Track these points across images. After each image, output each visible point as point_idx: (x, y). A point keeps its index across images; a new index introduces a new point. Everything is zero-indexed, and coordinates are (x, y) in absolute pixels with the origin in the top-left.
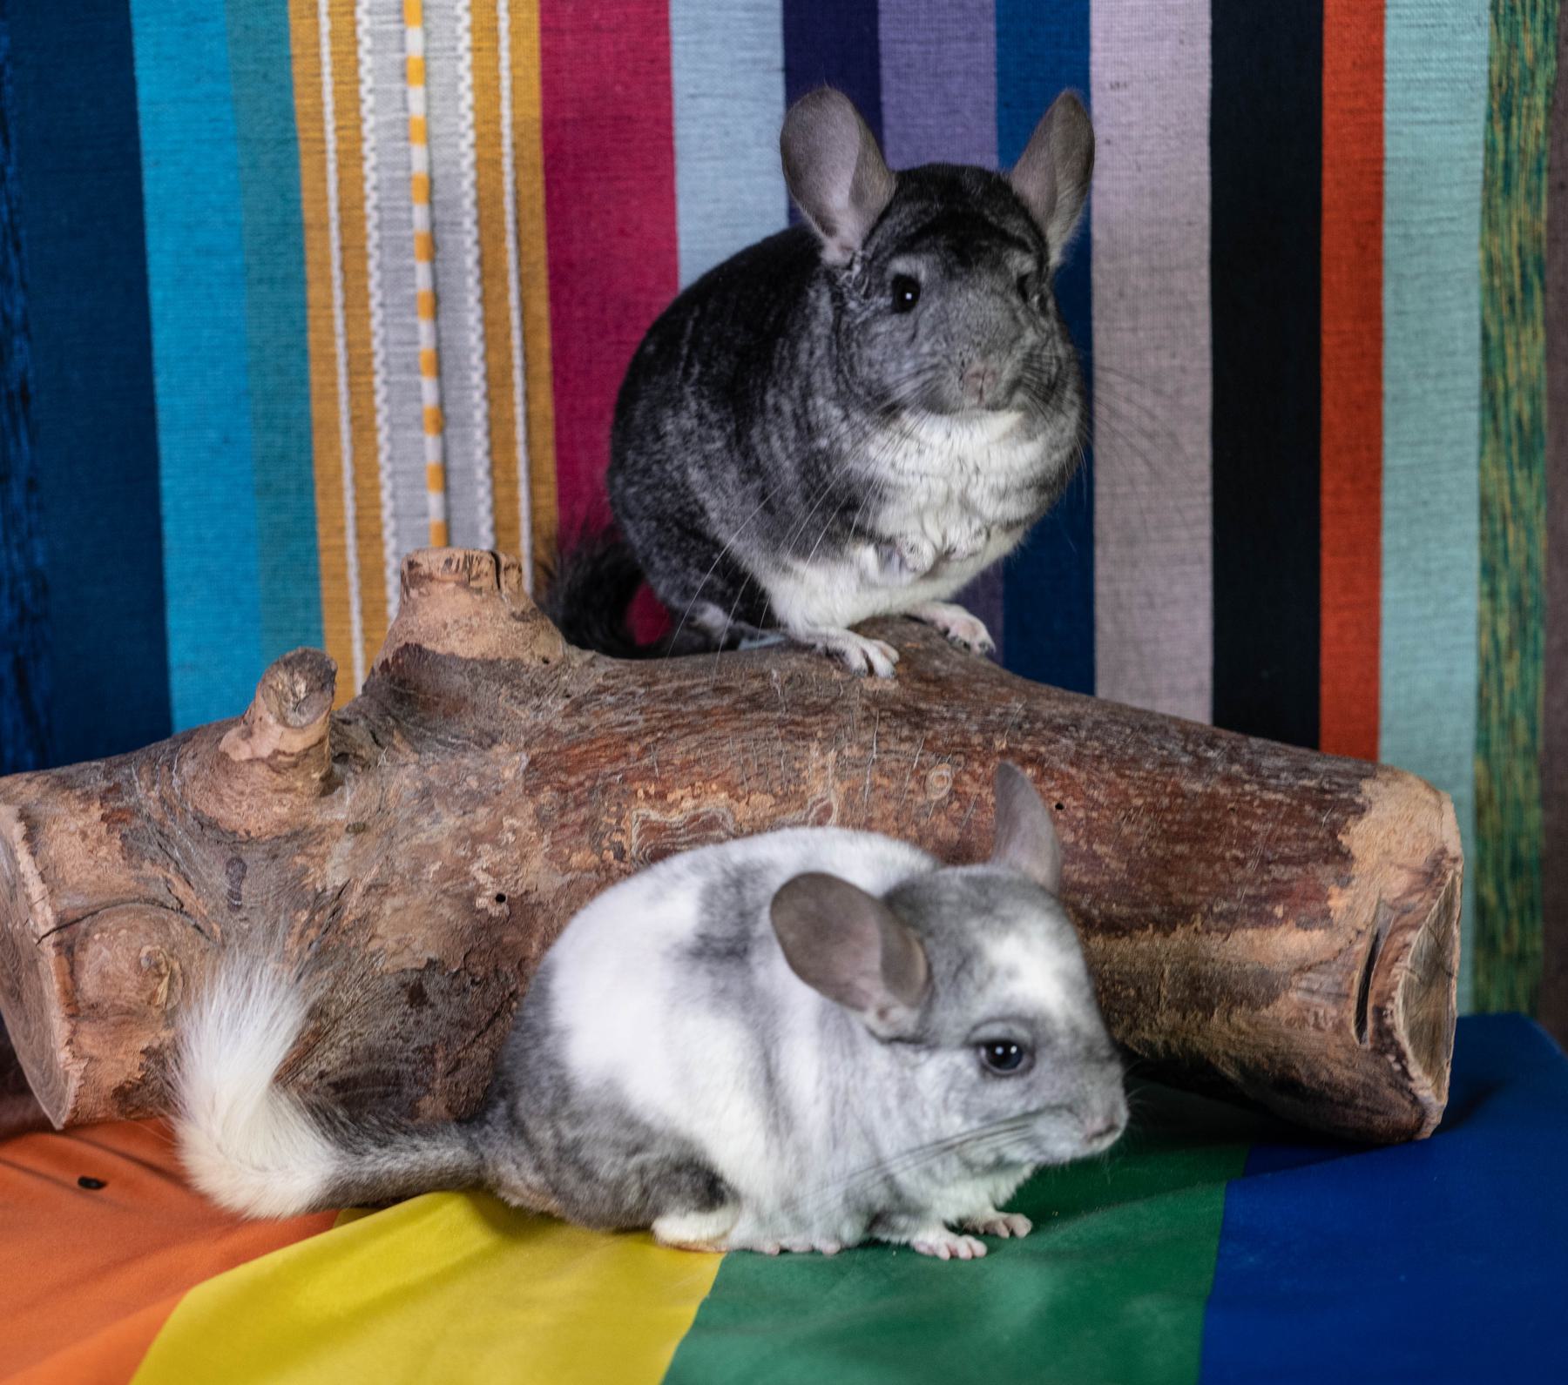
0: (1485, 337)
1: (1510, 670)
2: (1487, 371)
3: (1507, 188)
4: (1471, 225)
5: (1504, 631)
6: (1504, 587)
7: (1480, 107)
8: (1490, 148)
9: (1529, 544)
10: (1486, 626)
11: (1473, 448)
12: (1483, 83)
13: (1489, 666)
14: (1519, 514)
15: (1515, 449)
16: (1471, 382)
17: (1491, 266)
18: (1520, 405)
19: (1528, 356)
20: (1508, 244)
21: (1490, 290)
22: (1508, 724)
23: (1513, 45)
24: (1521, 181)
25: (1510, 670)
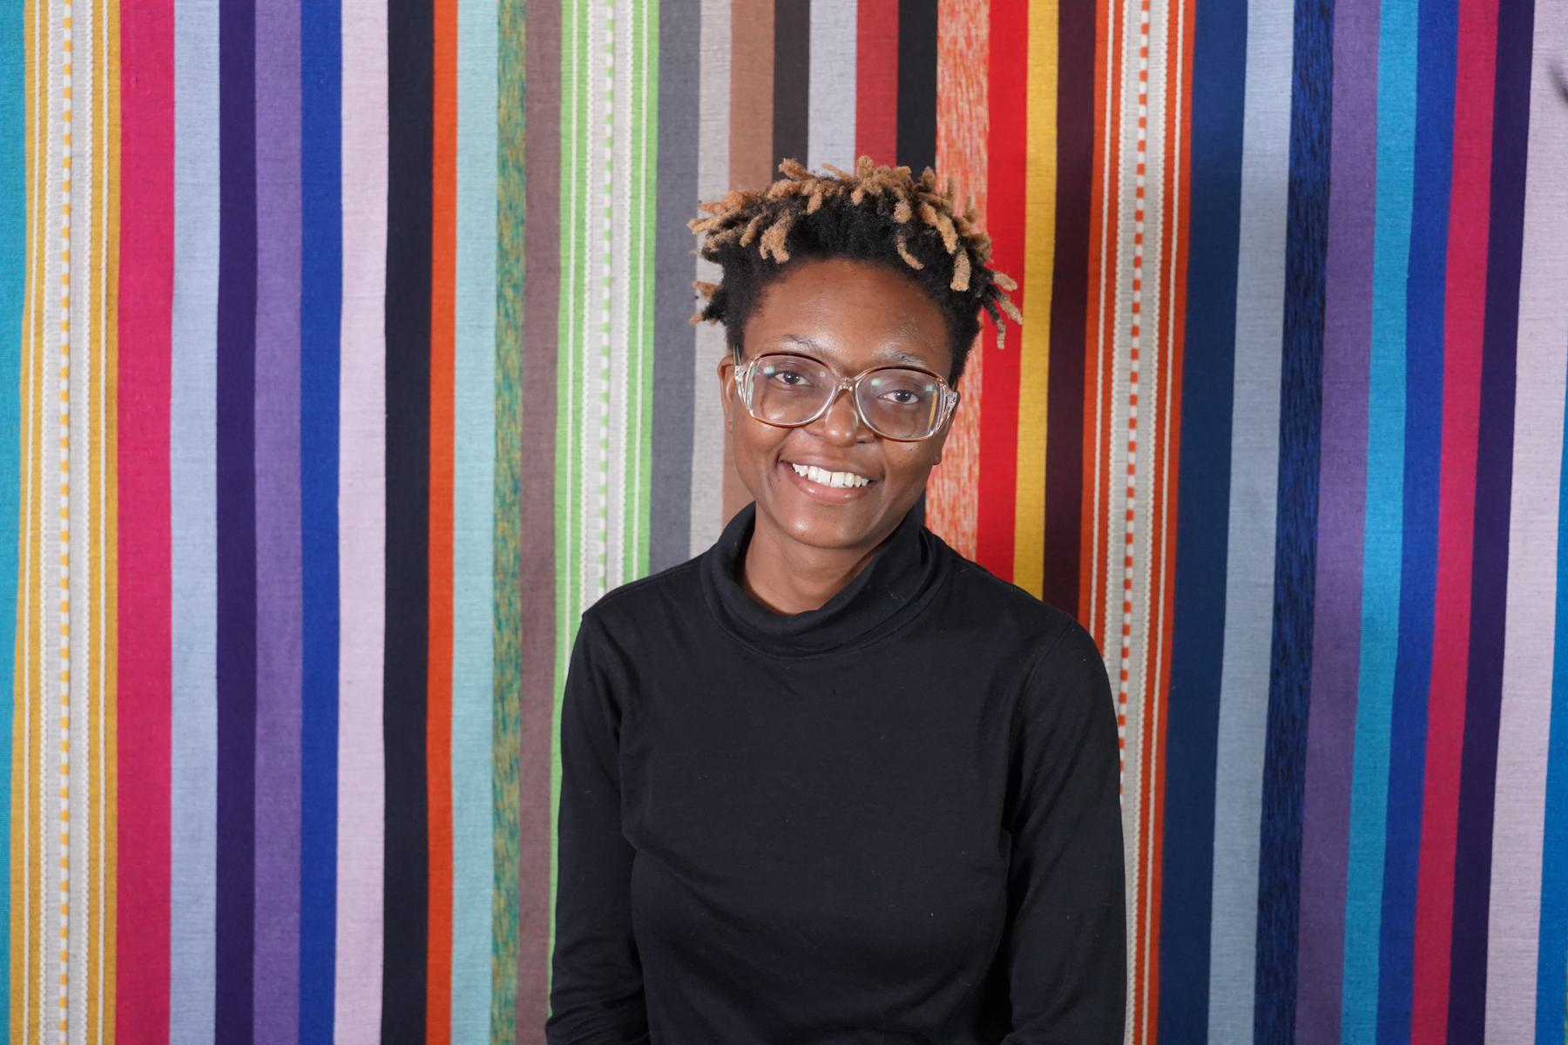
0: (494, 786)
1: (505, 921)
2: (495, 800)
3: (505, 729)
4: (488, 744)
5: (502, 904)
6: (503, 886)
7: (490, 697)
8: (495, 713)
9: (512, 870)
10: (495, 901)
11: (490, 829)
12: (491, 688)
13: (497, 919)
14: (509, 858)
15: (507, 834)
16: (489, 803)
17: (497, 759)
18: (509, 816)
19: (513, 796)
20: (505, 751)
21: (496, 770)
22: (506, 944)
23: (503, 674)
24: (511, 727)
25: (505, 921)
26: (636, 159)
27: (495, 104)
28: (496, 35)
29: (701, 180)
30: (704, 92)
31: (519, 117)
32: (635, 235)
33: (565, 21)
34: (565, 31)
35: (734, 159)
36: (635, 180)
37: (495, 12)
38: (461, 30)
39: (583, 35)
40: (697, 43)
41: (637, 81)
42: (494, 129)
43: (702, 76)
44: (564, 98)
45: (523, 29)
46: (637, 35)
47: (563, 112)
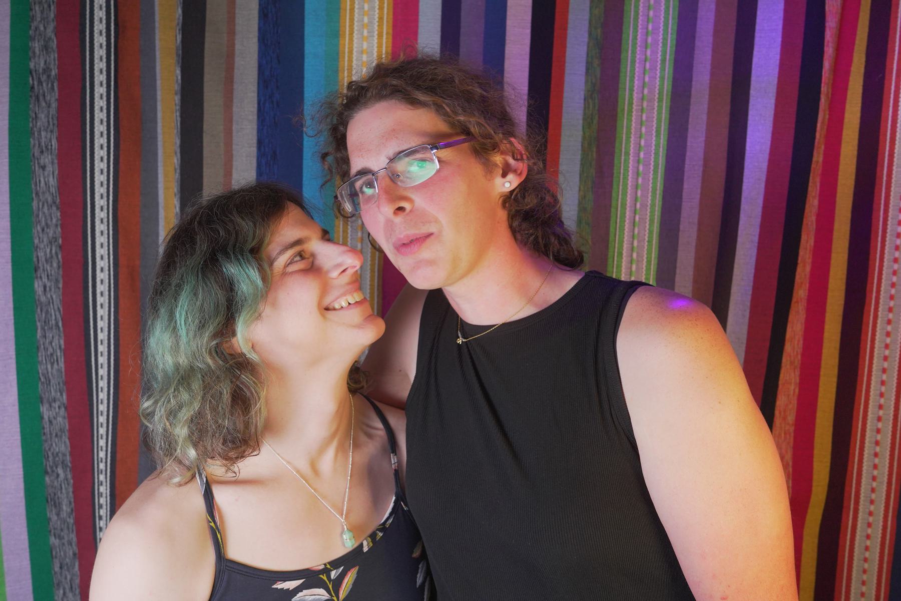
26: (652, 221)
27: (577, 189)
28: (580, 152)
29: (680, 233)
30: (685, 186)
31: (590, 196)
32: (649, 262)
33: (617, 145)
34: (617, 151)
35: (700, 223)
36: (651, 232)
37: (580, 139)
38: (562, 148)
39: (627, 154)
40: (683, 161)
41: (655, 179)
42: (577, 202)
43: (685, 178)
44: (615, 186)
45: (595, 150)
46: (656, 154)
47: (614, 195)
